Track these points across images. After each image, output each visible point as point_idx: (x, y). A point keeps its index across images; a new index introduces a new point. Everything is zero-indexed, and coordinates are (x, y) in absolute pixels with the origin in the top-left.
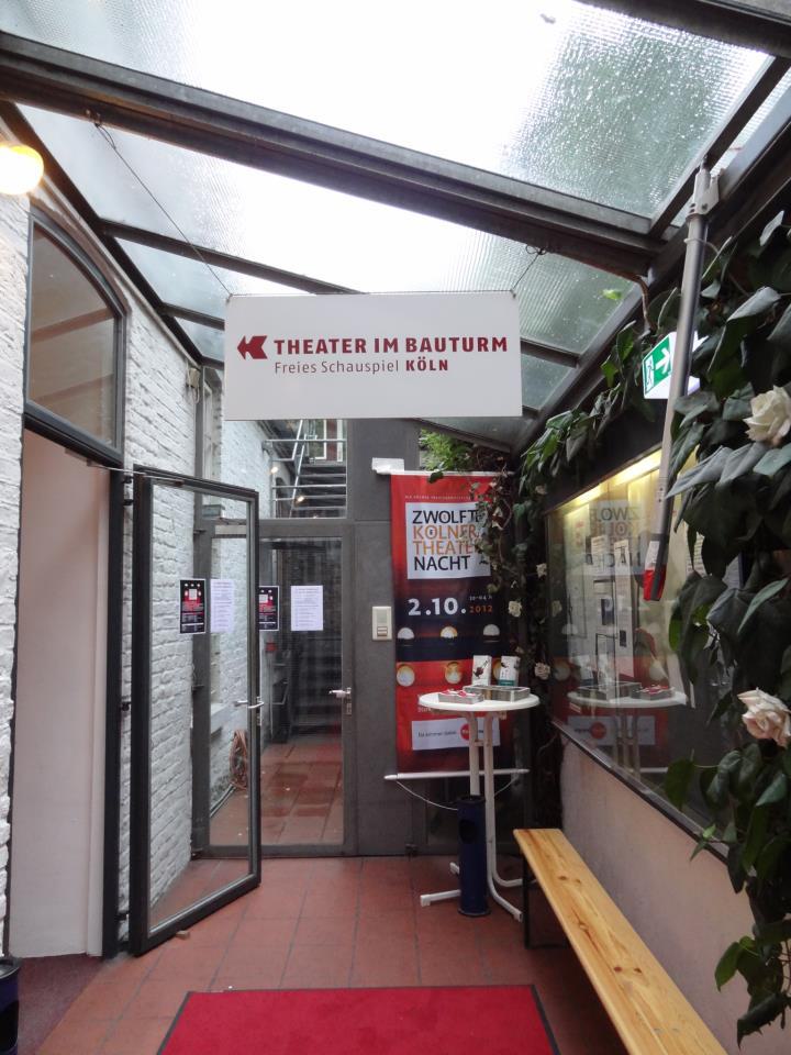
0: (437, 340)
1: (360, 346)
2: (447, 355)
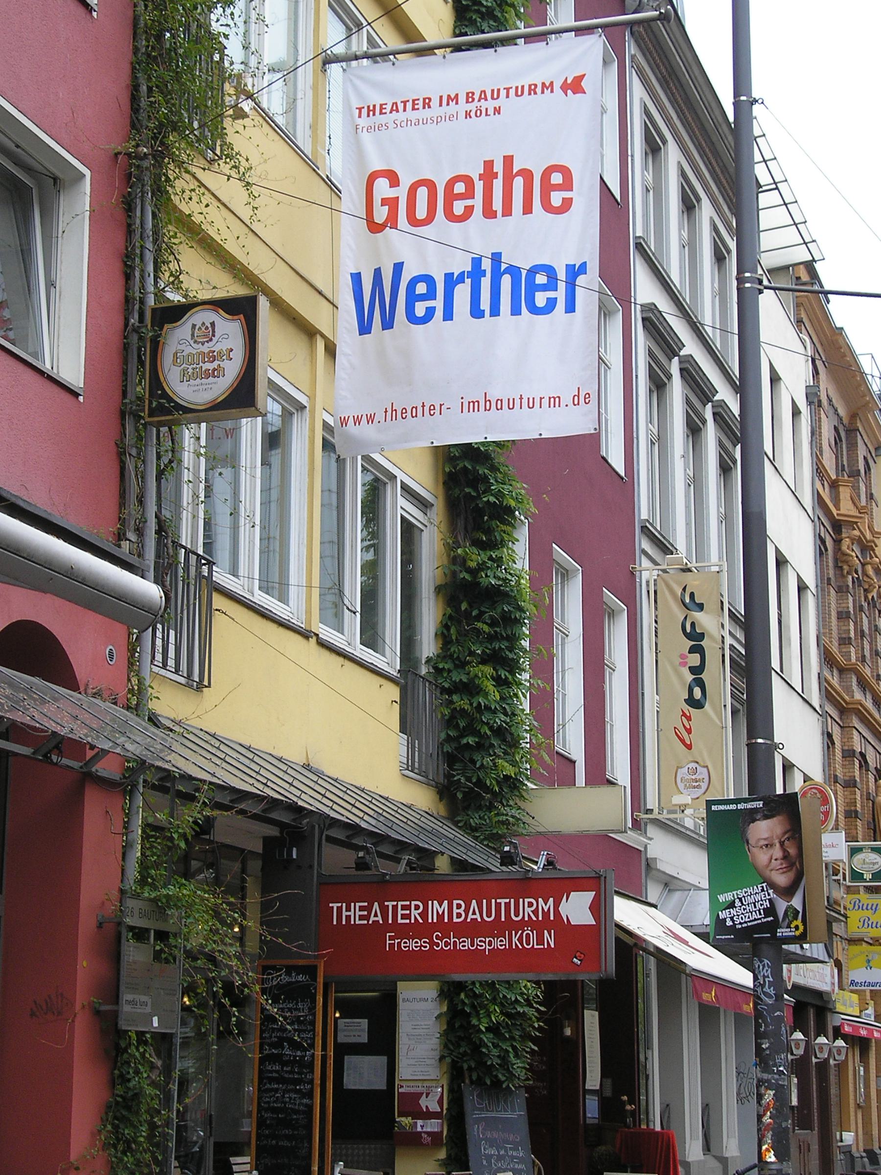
0: (493, 91)
1: (427, 102)
2: (502, 101)
